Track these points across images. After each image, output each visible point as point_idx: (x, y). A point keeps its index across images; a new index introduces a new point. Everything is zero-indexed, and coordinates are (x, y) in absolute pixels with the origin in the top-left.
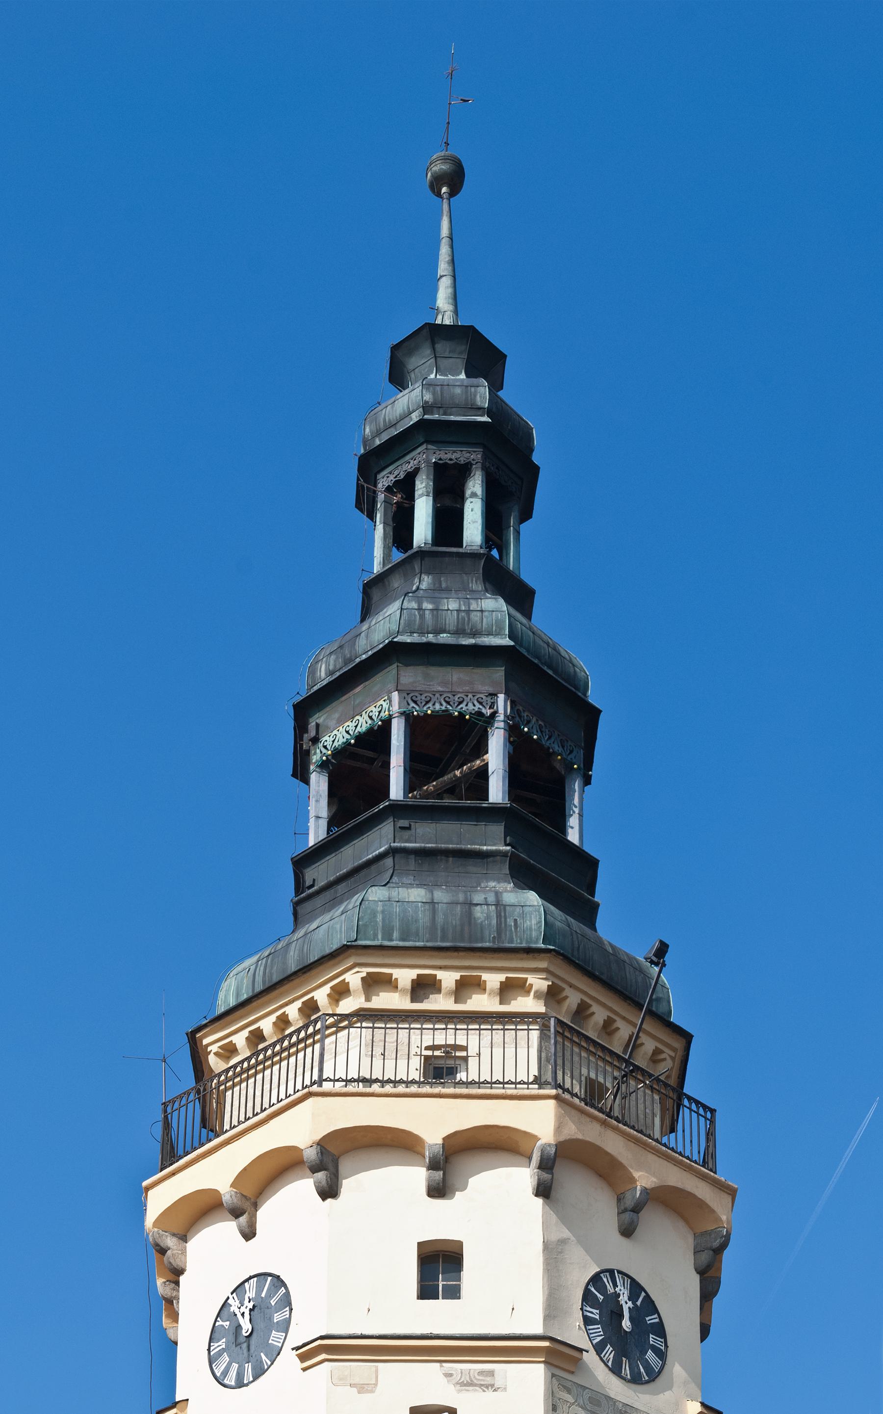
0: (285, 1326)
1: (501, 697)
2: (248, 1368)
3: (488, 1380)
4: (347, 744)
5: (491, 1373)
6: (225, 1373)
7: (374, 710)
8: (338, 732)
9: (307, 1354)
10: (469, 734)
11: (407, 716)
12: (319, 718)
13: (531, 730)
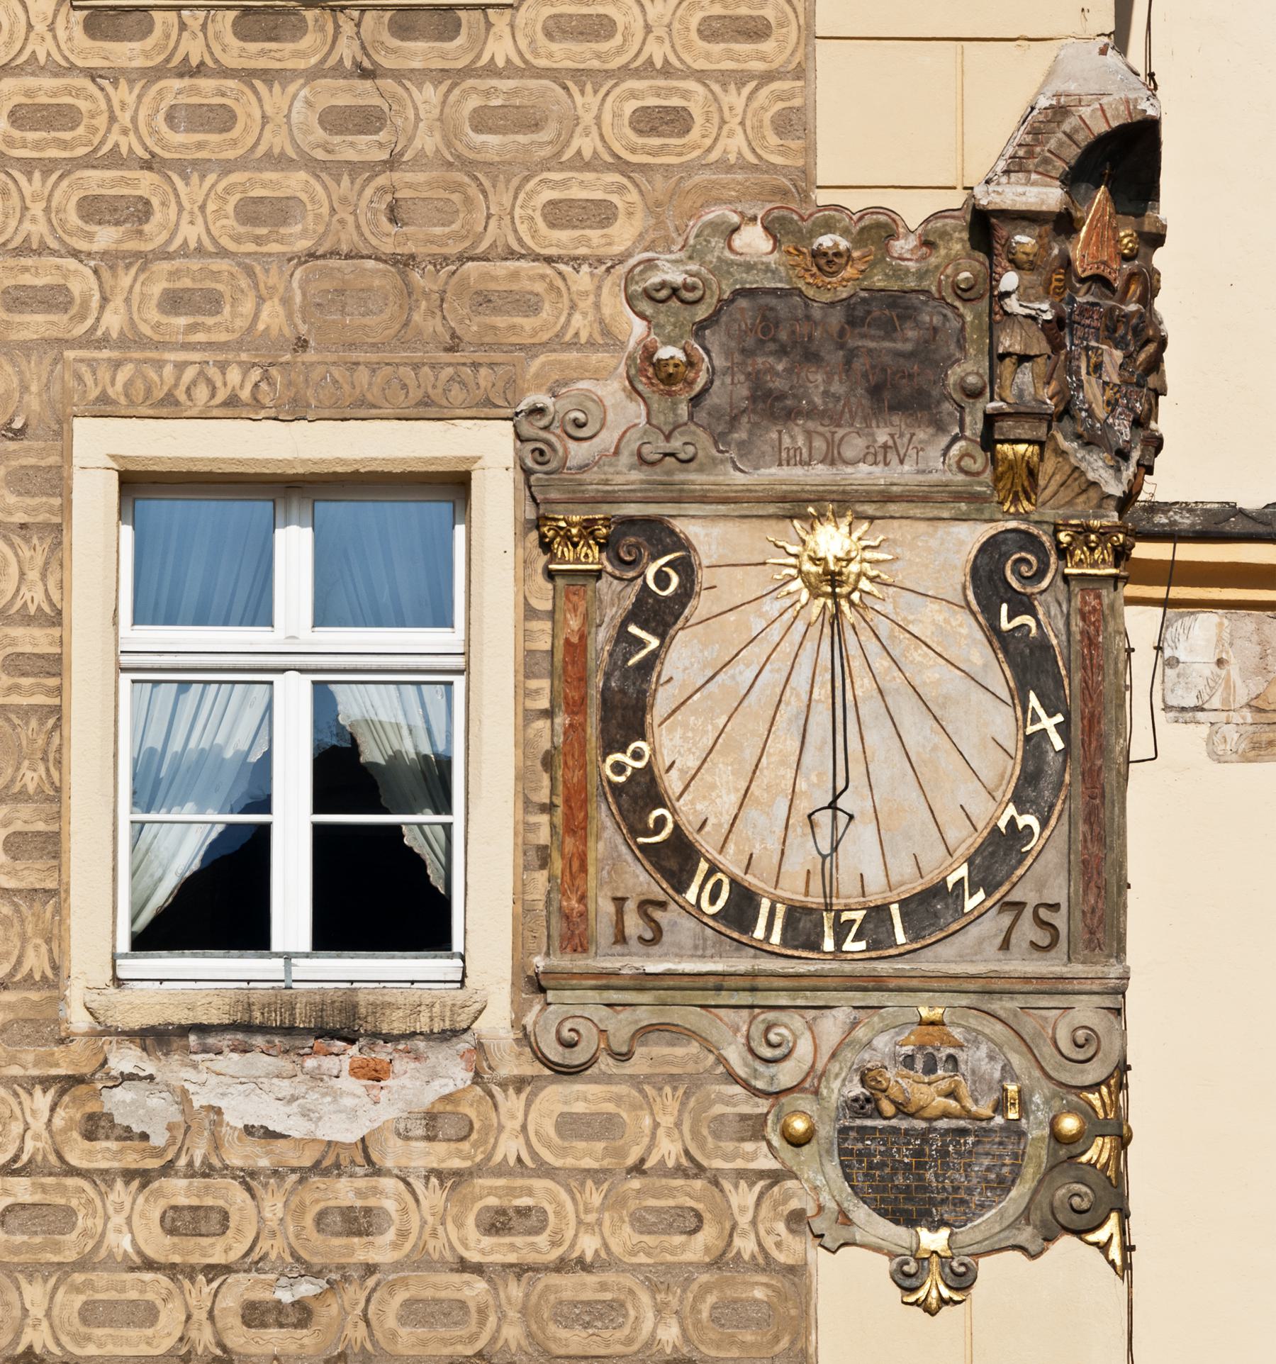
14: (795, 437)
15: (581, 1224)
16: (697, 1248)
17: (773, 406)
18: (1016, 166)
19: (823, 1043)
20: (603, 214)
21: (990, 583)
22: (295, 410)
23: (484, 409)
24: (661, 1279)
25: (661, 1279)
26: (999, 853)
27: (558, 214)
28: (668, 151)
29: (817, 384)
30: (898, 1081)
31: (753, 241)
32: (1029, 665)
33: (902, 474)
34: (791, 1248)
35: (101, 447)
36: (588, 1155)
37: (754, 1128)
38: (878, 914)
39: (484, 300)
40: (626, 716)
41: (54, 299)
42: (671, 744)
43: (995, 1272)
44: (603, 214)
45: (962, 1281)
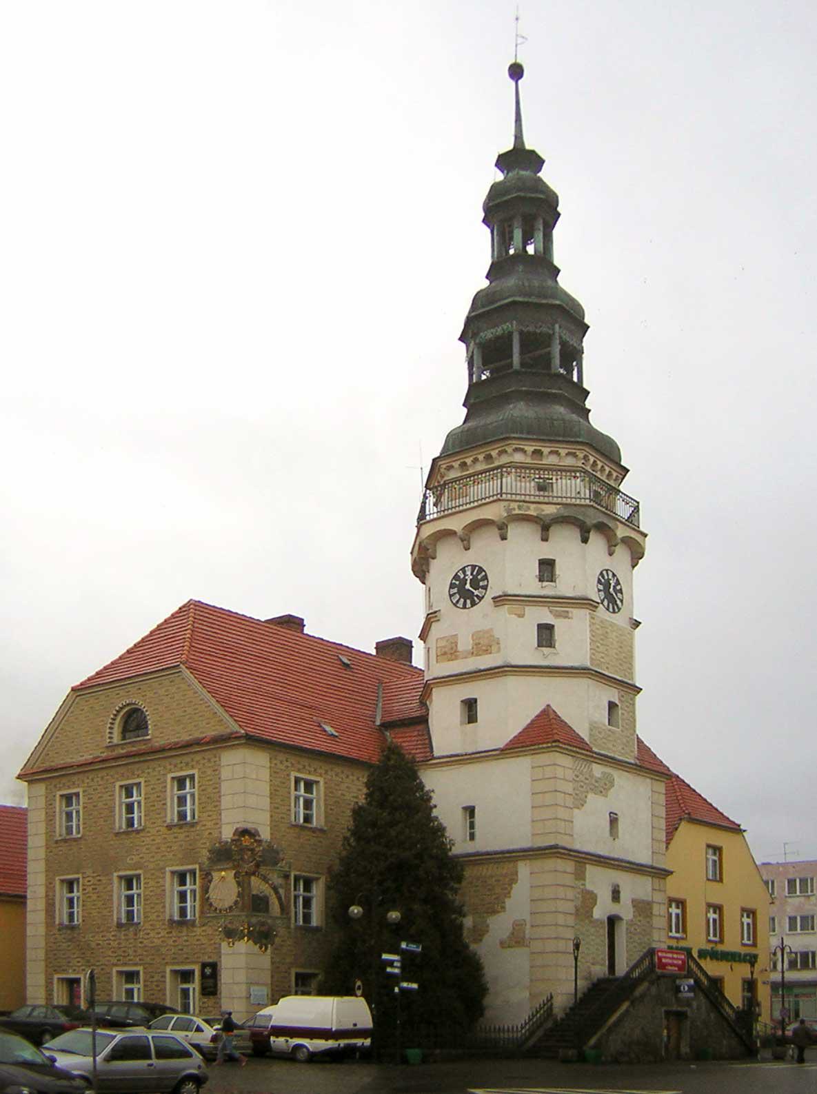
2: (468, 601)
6: (458, 602)
9: (500, 600)
15: (204, 940)
17: (219, 860)
18: (234, 835)
21: (236, 876)
22: (182, 865)
23: (196, 863)
26: (236, 903)
27: (202, 844)
28: (211, 836)
30: (229, 926)
32: (239, 884)
33: (228, 866)
37: (217, 930)
38: (226, 910)
39: (196, 853)
40: (207, 892)
43: (236, 943)
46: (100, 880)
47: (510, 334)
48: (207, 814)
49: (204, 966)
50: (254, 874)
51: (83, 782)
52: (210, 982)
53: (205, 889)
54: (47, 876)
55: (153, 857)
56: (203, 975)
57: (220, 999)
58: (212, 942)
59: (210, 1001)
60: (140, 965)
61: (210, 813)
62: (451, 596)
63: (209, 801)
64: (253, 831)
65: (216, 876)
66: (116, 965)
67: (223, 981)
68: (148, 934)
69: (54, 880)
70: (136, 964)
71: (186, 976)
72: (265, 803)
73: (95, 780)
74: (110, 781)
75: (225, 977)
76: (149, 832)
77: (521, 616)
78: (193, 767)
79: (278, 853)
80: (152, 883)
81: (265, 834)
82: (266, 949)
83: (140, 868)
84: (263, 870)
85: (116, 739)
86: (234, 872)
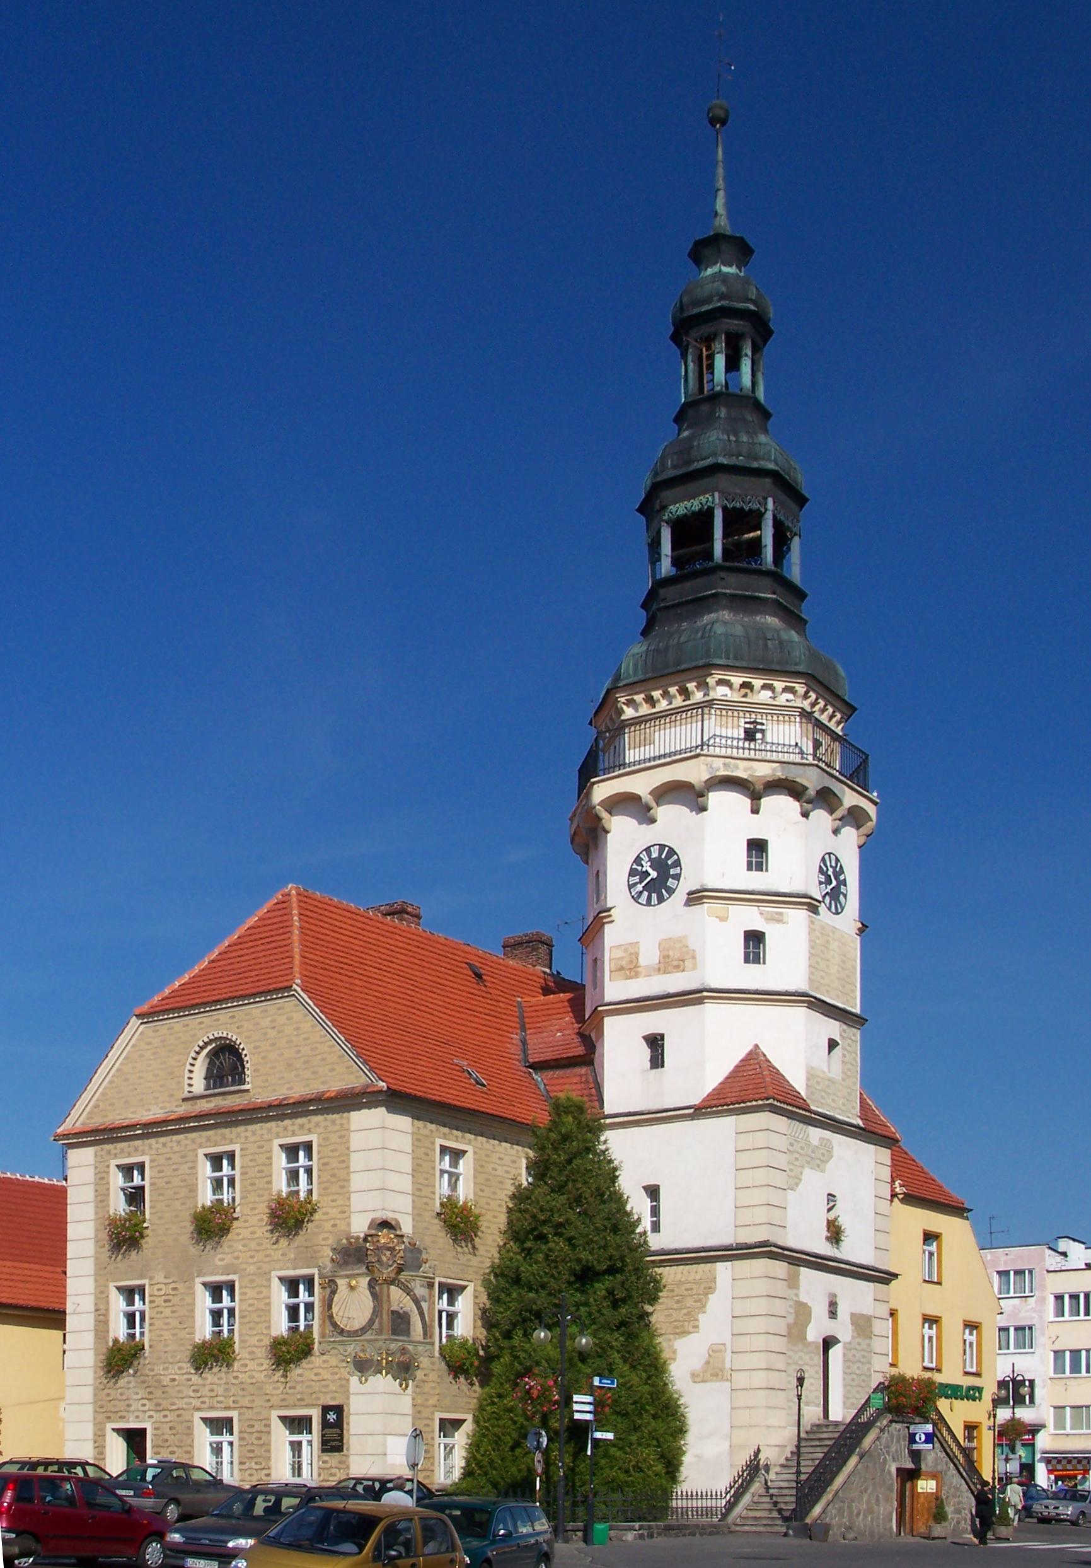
0: (677, 877)
1: (770, 501)
3: (780, 918)
4: (685, 516)
5: (781, 914)
7: (703, 499)
8: (679, 509)
10: (753, 520)
11: (725, 509)
12: (667, 494)
13: (781, 517)
14: (349, 1267)
15: (326, 1374)
16: (337, 1377)
17: (346, 1263)
19: (351, 1349)
20: (327, 1239)
24: (334, 1381)
25: (334, 1381)
29: (351, 1259)
31: (344, 1241)
34: (347, 1376)
35: (273, 1273)
36: (325, 1365)
37: (343, 1361)
39: (315, 1252)
41: (269, 1256)
42: (335, 1310)
44: (327, 1239)
45: (366, 1380)
46: (175, 1289)
47: (708, 513)
48: (330, 1197)
49: (326, 1409)
50: (392, 1282)
51: (150, 1148)
52: (332, 1433)
53: (328, 1304)
54: (96, 1281)
55: (252, 1257)
56: (325, 1424)
57: (347, 1456)
58: (337, 1377)
59: (333, 1459)
60: (234, 1409)
61: (335, 1197)
62: (630, 887)
63: (333, 1179)
64: (393, 1223)
65: (342, 1283)
66: (198, 1409)
67: (352, 1431)
68: (246, 1365)
69: (107, 1287)
70: (228, 1408)
71: (298, 1424)
72: (406, 1183)
73: (169, 1144)
74: (189, 1148)
75: (354, 1426)
76: (246, 1221)
77: (723, 919)
78: (310, 1131)
79: (420, 1252)
80: (251, 1293)
81: (407, 1228)
82: (407, 1386)
83: (235, 1273)
84: (402, 1277)
85: (199, 1085)
86: (368, 1279)
